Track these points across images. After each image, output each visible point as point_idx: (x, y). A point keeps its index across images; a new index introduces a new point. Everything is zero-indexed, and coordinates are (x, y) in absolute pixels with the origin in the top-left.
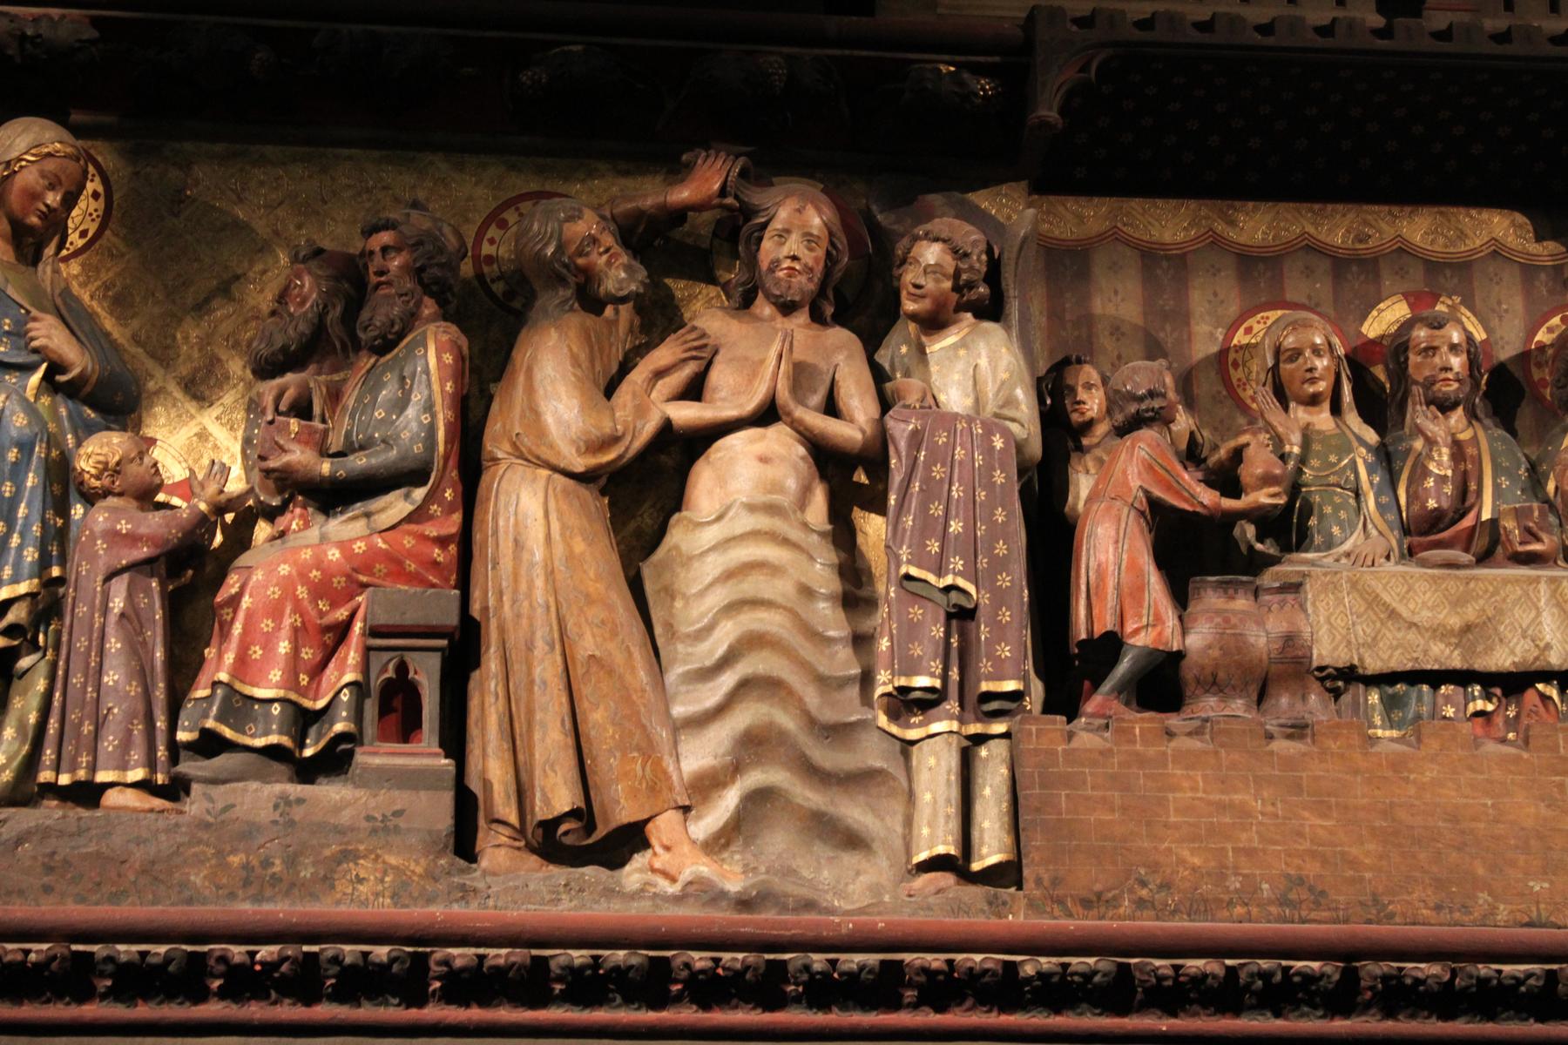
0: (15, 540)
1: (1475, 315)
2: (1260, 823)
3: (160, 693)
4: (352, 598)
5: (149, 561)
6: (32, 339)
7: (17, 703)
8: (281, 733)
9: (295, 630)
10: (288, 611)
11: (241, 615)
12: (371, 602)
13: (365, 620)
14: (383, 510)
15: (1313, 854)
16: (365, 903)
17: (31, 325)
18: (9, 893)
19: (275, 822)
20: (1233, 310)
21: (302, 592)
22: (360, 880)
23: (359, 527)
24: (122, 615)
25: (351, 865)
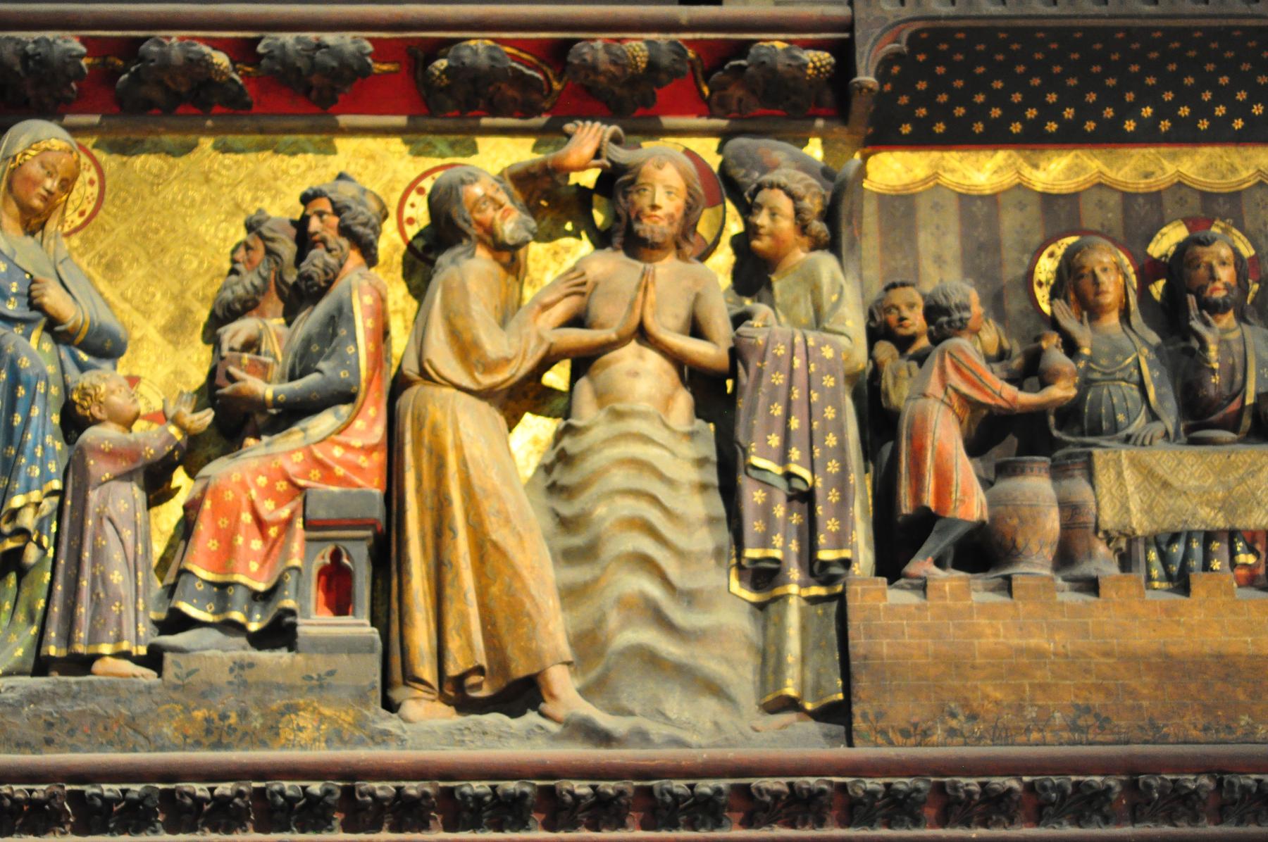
1: (1246, 235)
2: (1053, 663)
15: (1098, 688)
19: (230, 683)
20: (1037, 238)
22: (300, 729)
25: (293, 716)
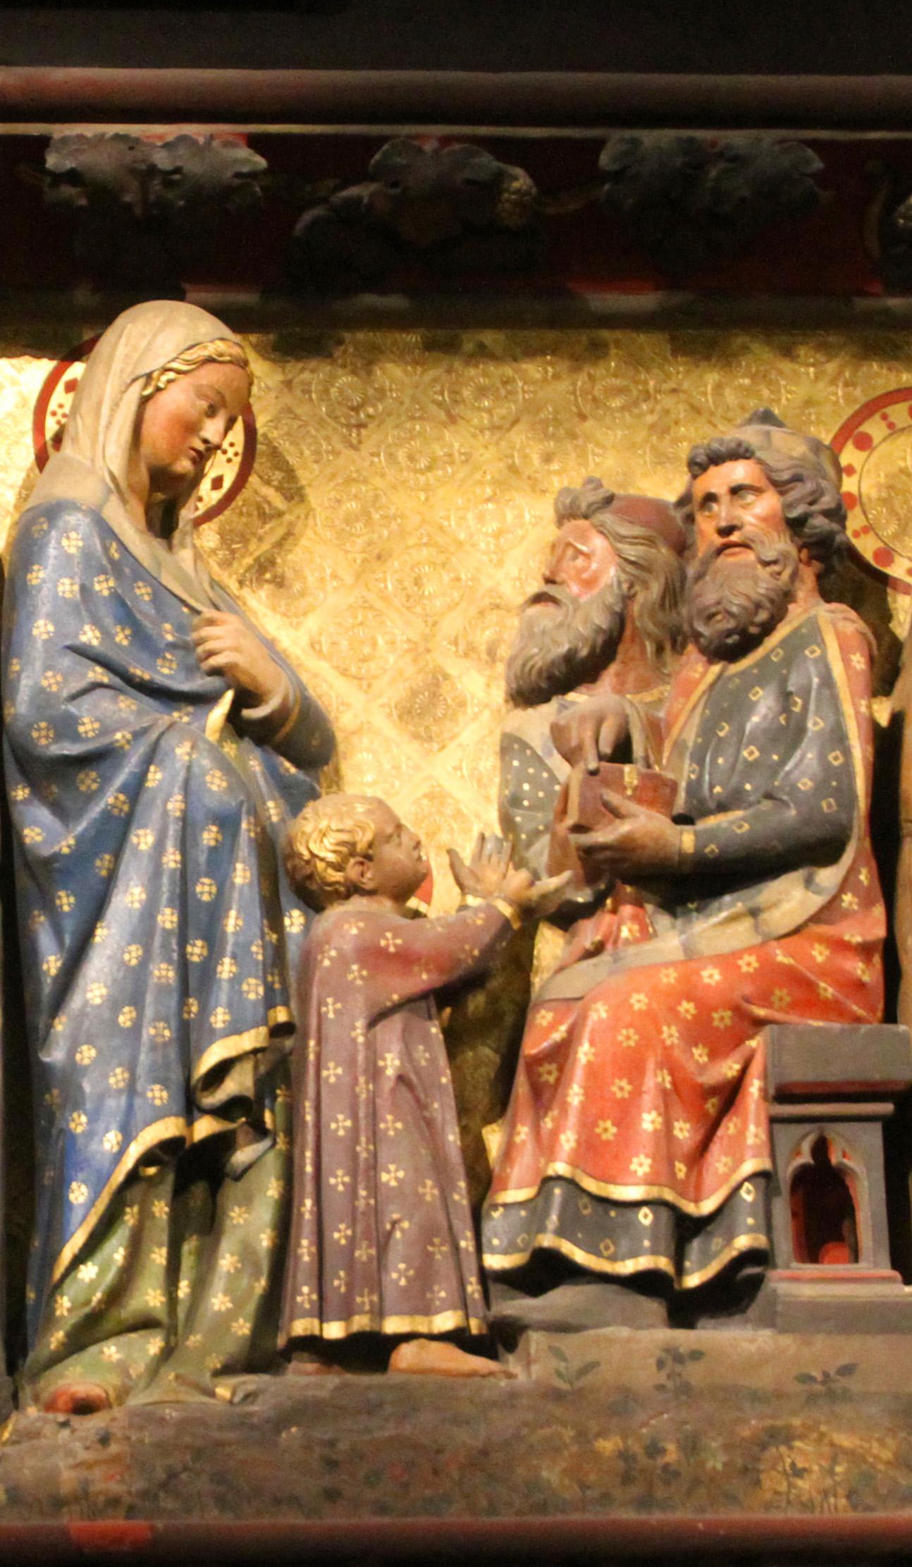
0: (226, 969)
3: (461, 1196)
4: (739, 1041)
5: (423, 996)
6: (211, 654)
7: (236, 1216)
8: (654, 1251)
9: (664, 1093)
10: (651, 1065)
11: (579, 1074)
12: (776, 1048)
13: (765, 1077)
14: (775, 905)
16: (808, 1506)
17: (206, 631)
18: (277, 1502)
19: (661, 1388)
21: (671, 1034)
22: (799, 1473)
23: (741, 935)
24: (401, 1078)
25: (783, 1449)
